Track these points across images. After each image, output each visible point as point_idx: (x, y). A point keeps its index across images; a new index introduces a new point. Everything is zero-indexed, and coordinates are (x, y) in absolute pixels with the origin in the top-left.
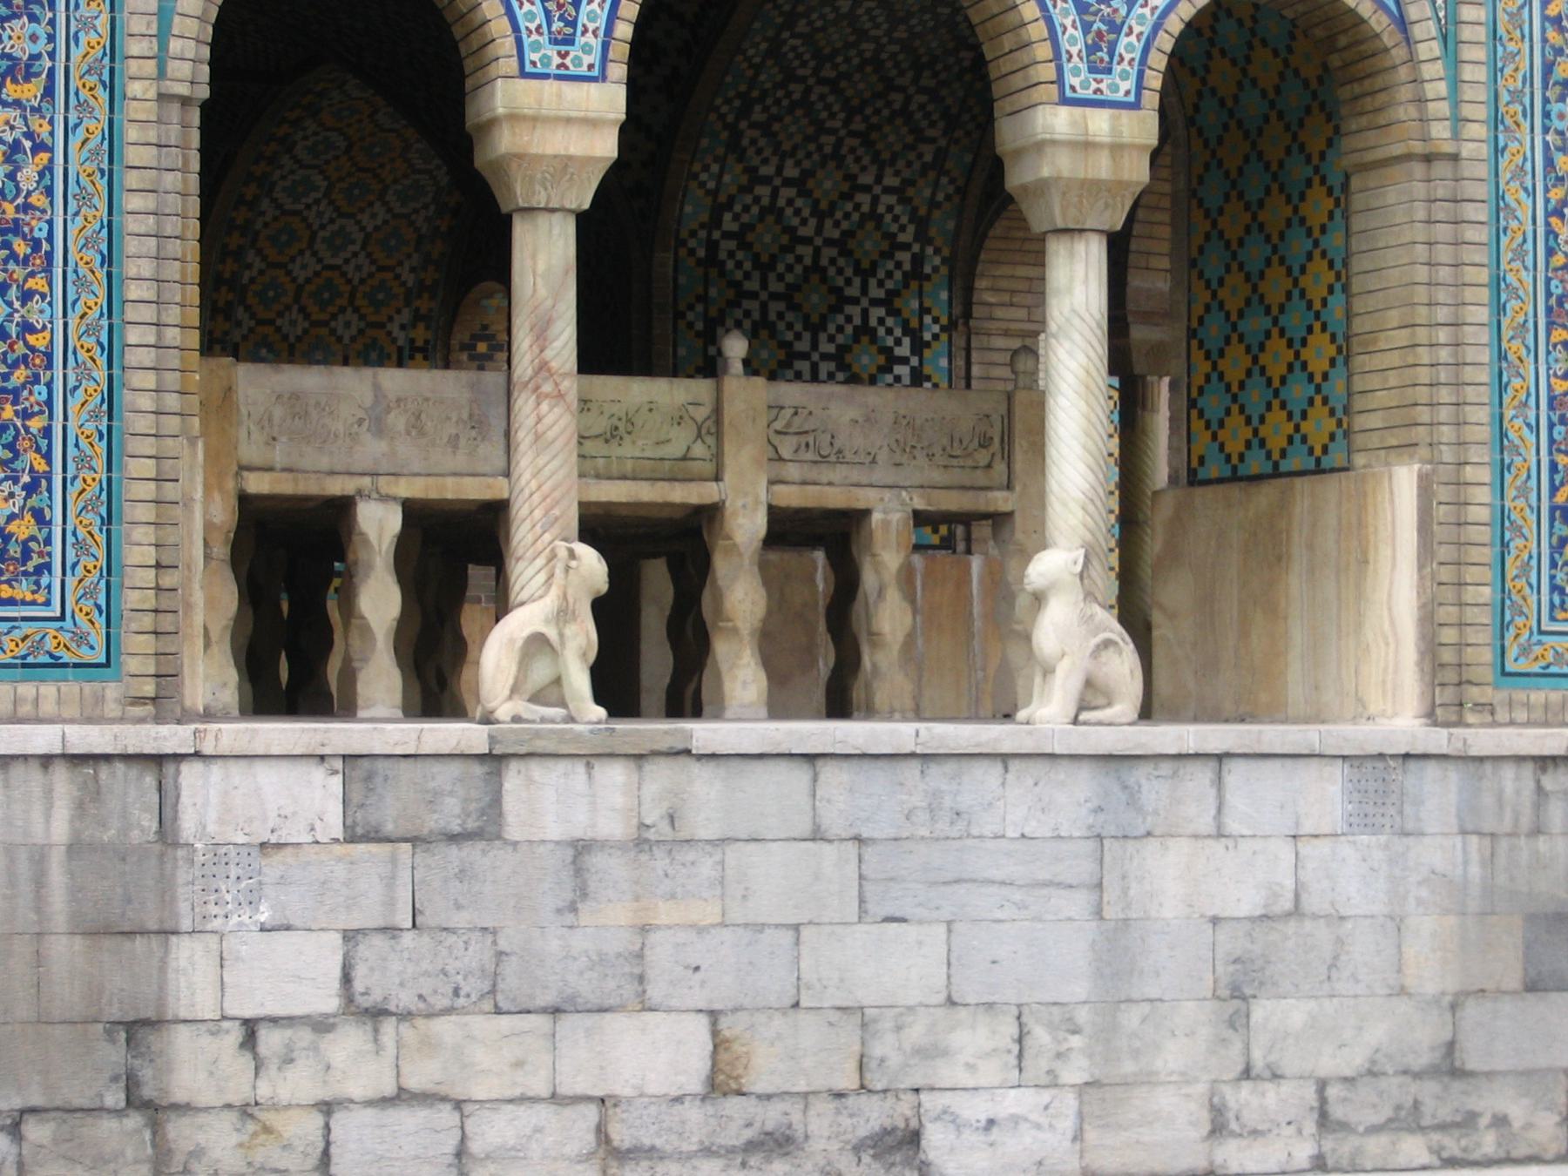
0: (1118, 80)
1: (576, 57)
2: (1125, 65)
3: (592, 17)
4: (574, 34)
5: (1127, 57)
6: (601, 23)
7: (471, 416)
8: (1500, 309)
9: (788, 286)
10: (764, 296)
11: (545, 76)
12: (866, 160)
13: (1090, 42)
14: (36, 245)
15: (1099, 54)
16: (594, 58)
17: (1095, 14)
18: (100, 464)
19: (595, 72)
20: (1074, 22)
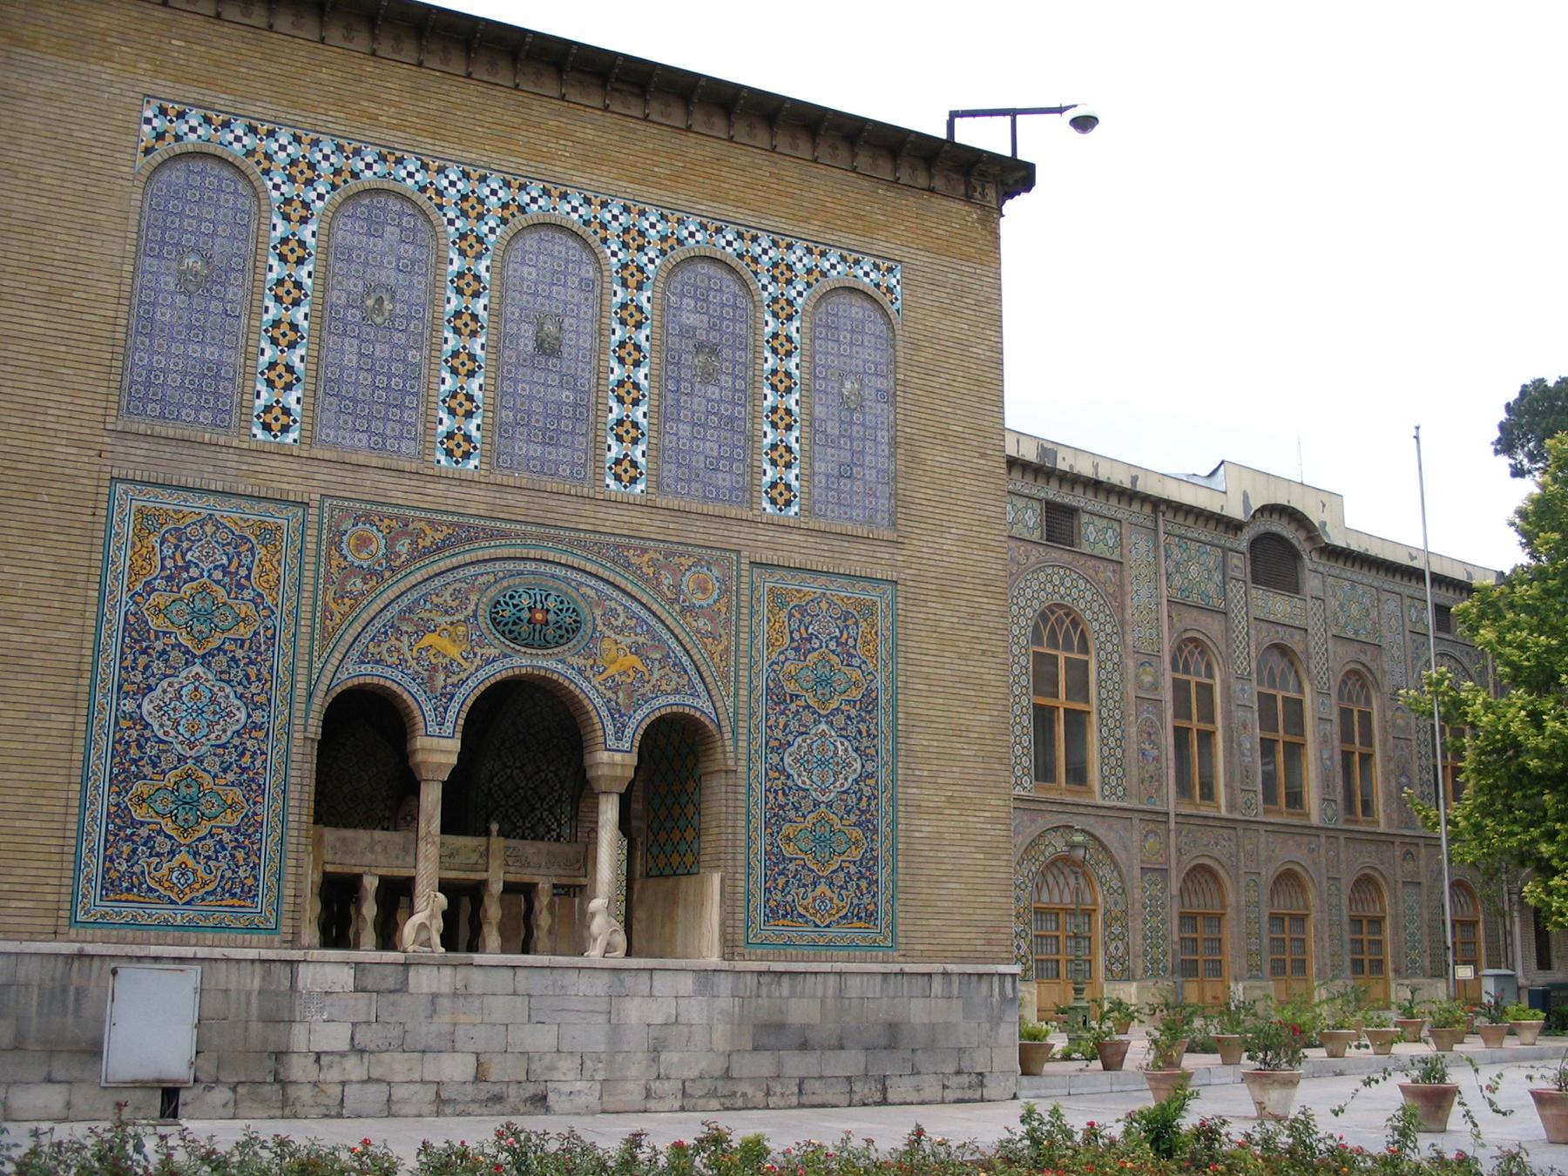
14: (260, 786)
18: (277, 861)
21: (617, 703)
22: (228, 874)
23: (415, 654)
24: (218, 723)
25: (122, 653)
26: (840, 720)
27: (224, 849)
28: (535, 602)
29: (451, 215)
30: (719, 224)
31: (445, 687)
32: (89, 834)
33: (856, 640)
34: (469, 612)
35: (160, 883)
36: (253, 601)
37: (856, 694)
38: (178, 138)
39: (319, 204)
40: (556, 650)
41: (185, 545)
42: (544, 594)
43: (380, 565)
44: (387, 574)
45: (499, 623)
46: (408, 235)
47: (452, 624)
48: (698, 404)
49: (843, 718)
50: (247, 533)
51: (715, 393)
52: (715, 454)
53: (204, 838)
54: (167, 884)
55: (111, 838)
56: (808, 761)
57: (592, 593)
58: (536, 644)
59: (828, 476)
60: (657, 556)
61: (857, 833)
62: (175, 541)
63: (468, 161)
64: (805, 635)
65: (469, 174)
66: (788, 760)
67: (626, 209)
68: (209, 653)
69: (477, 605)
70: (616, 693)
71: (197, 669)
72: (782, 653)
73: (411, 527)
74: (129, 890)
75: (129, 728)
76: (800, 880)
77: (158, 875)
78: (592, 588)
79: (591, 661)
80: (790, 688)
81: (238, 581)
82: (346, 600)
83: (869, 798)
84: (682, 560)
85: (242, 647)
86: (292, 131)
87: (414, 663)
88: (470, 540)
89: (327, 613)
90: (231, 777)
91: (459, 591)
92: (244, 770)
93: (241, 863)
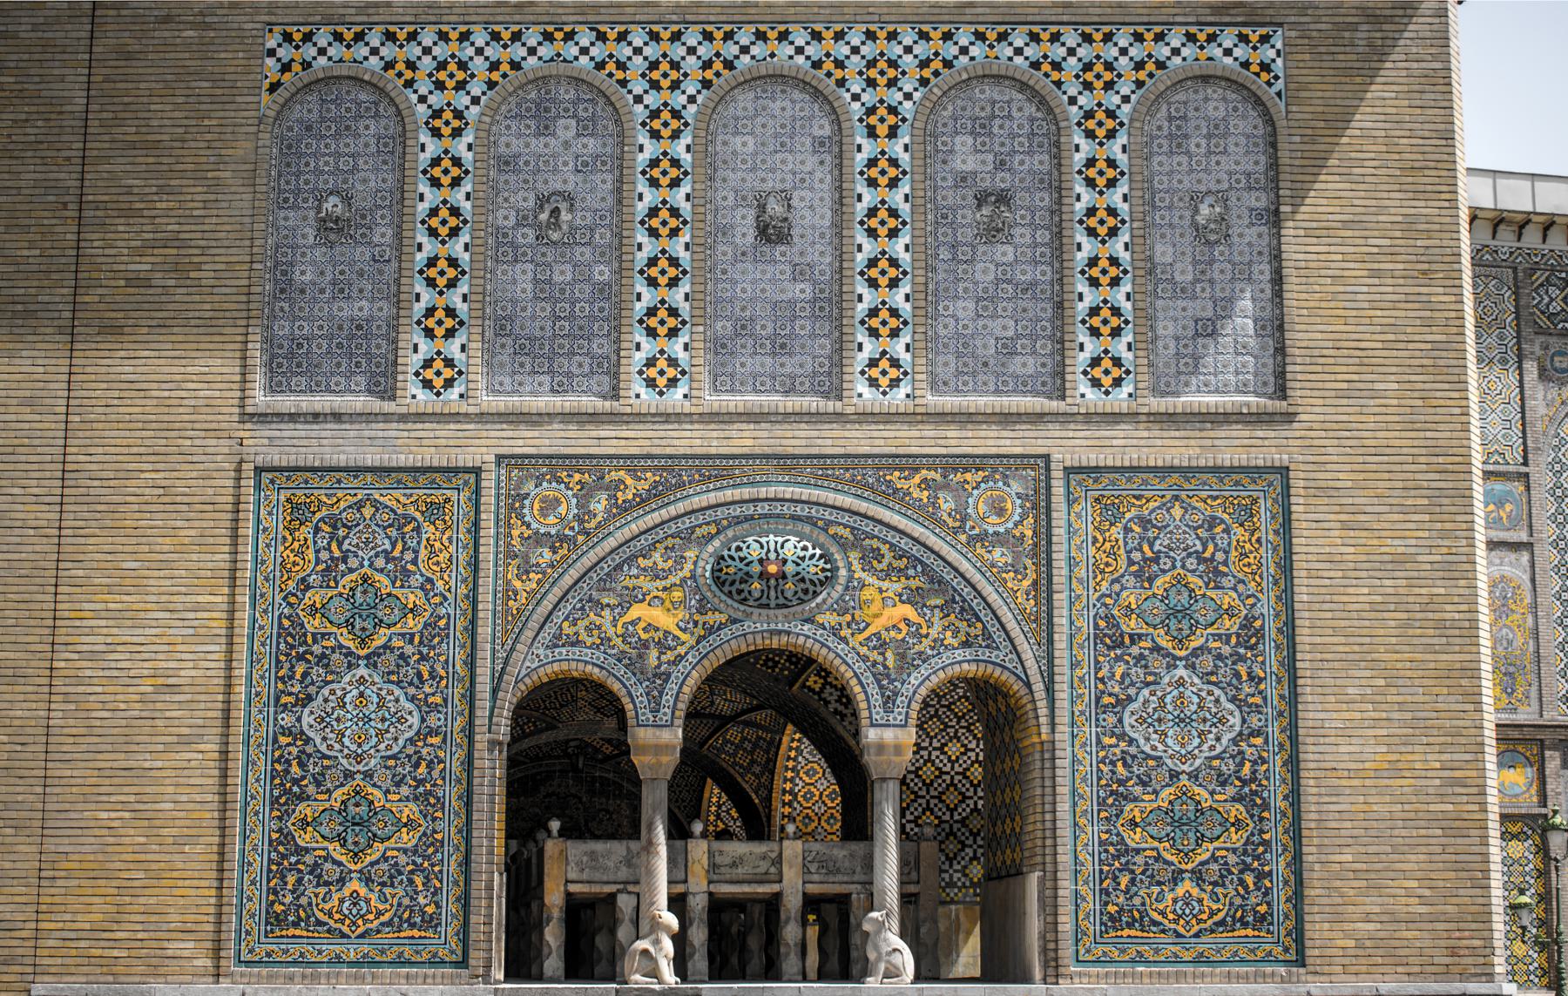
8: (1075, 804)
16: (669, 717)
21: (885, 667)
22: (406, 901)
24: (387, 731)
25: (278, 661)
26: (1207, 662)
27: (400, 873)
29: (638, 90)
30: (1001, 29)
31: (659, 666)
32: (250, 864)
33: (1226, 552)
35: (330, 915)
36: (422, 588)
37: (1230, 625)
38: (306, 65)
39: (475, 110)
41: (341, 532)
42: (780, 540)
43: (572, 528)
44: (581, 538)
45: (723, 583)
46: (586, 128)
47: (665, 589)
48: (985, 274)
49: (1210, 658)
50: (411, 510)
51: (1005, 253)
52: (1010, 333)
53: (377, 862)
54: (337, 916)
55: (274, 868)
56: (1159, 720)
57: (846, 533)
59: (1177, 339)
60: (931, 475)
61: (1237, 811)
62: (329, 529)
63: (656, 18)
64: (1149, 554)
65: (658, 34)
66: (1128, 720)
67: (871, 36)
68: (373, 653)
69: (695, 563)
70: (883, 654)
71: (362, 671)
72: (1113, 582)
74: (295, 925)
75: (289, 745)
76: (1152, 876)
77: (327, 907)
78: (846, 526)
79: (848, 618)
80: (1132, 625)
81: (404, 568)
82: (532, 575)
83: (1254, 763)
84: (968, 476)
85: (411, 642)
86: (436, 28)
89: (510, 593)
90: (405, 790)
92: (421, 782)
93: (420, 888)
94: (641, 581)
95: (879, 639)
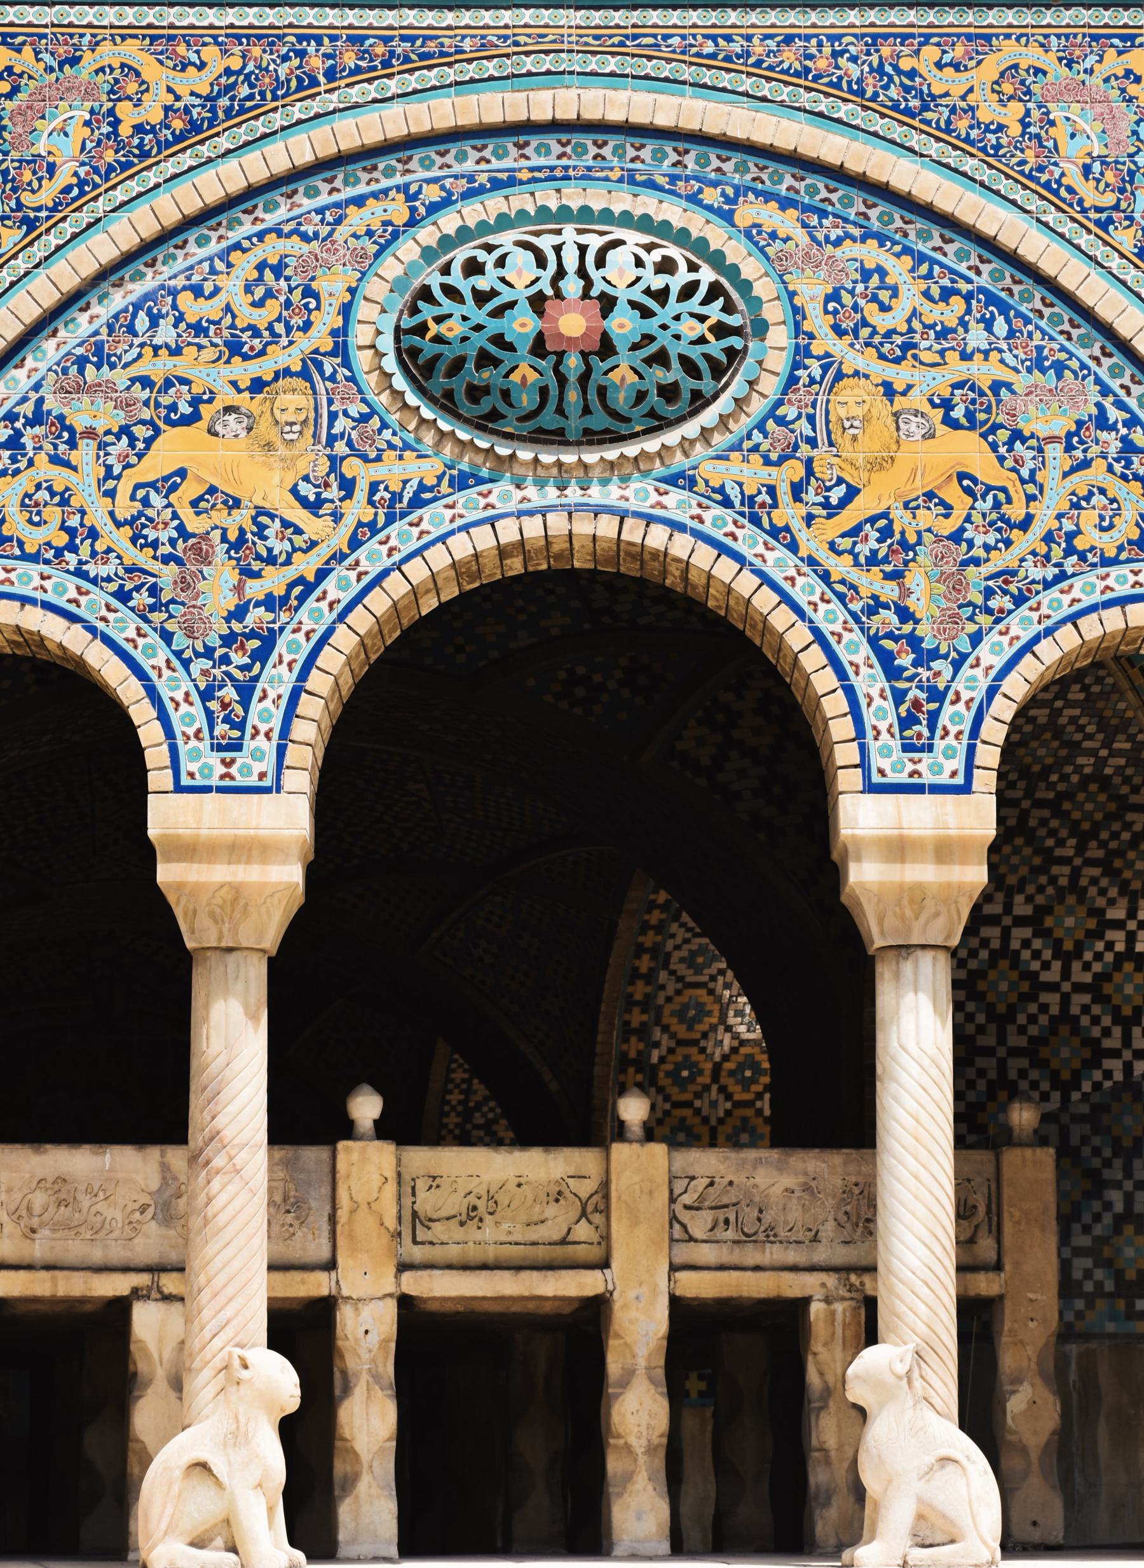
0: (941, 759)
1: (244, 765)
2: (950, 740)
3: (265, 716)
4: (242, 738)
5: (953, 730)
6: (276, 723)
7: (285, 1199)
9: (1032, 1039)
10: (1001, 1052)
11: (206, 789)
12: (1113, 892)
13: (904, 714)
15: (916, 728)
16: (268, 764)
17: (910, 679)
19: (267, 782)
20: (882, 690)
21: (905, 615)
23: (125, 508)
28: (561, 273)
31: (239, 613)
34: (320, 337)
40: (652, 445)
42: (595, 242)
45: (429, 368)
47: (257, 386)
57: (786, 222)
58: (574, 424)
60: (1031, 55)
69: (346, 310)
70: (896, 576)
73: (89, 62)
79: (794, 470)
87: (120, 539)
88: (307, 83)
91: (278, 270)
94: (181, 366)
95: (886, 533)
